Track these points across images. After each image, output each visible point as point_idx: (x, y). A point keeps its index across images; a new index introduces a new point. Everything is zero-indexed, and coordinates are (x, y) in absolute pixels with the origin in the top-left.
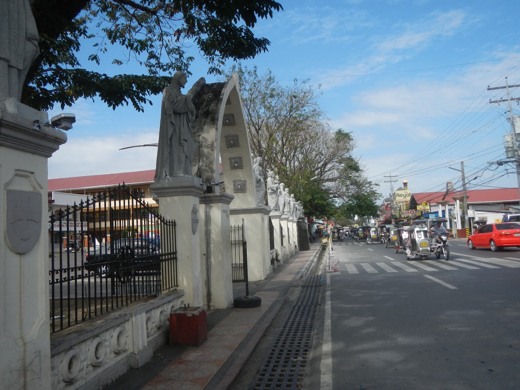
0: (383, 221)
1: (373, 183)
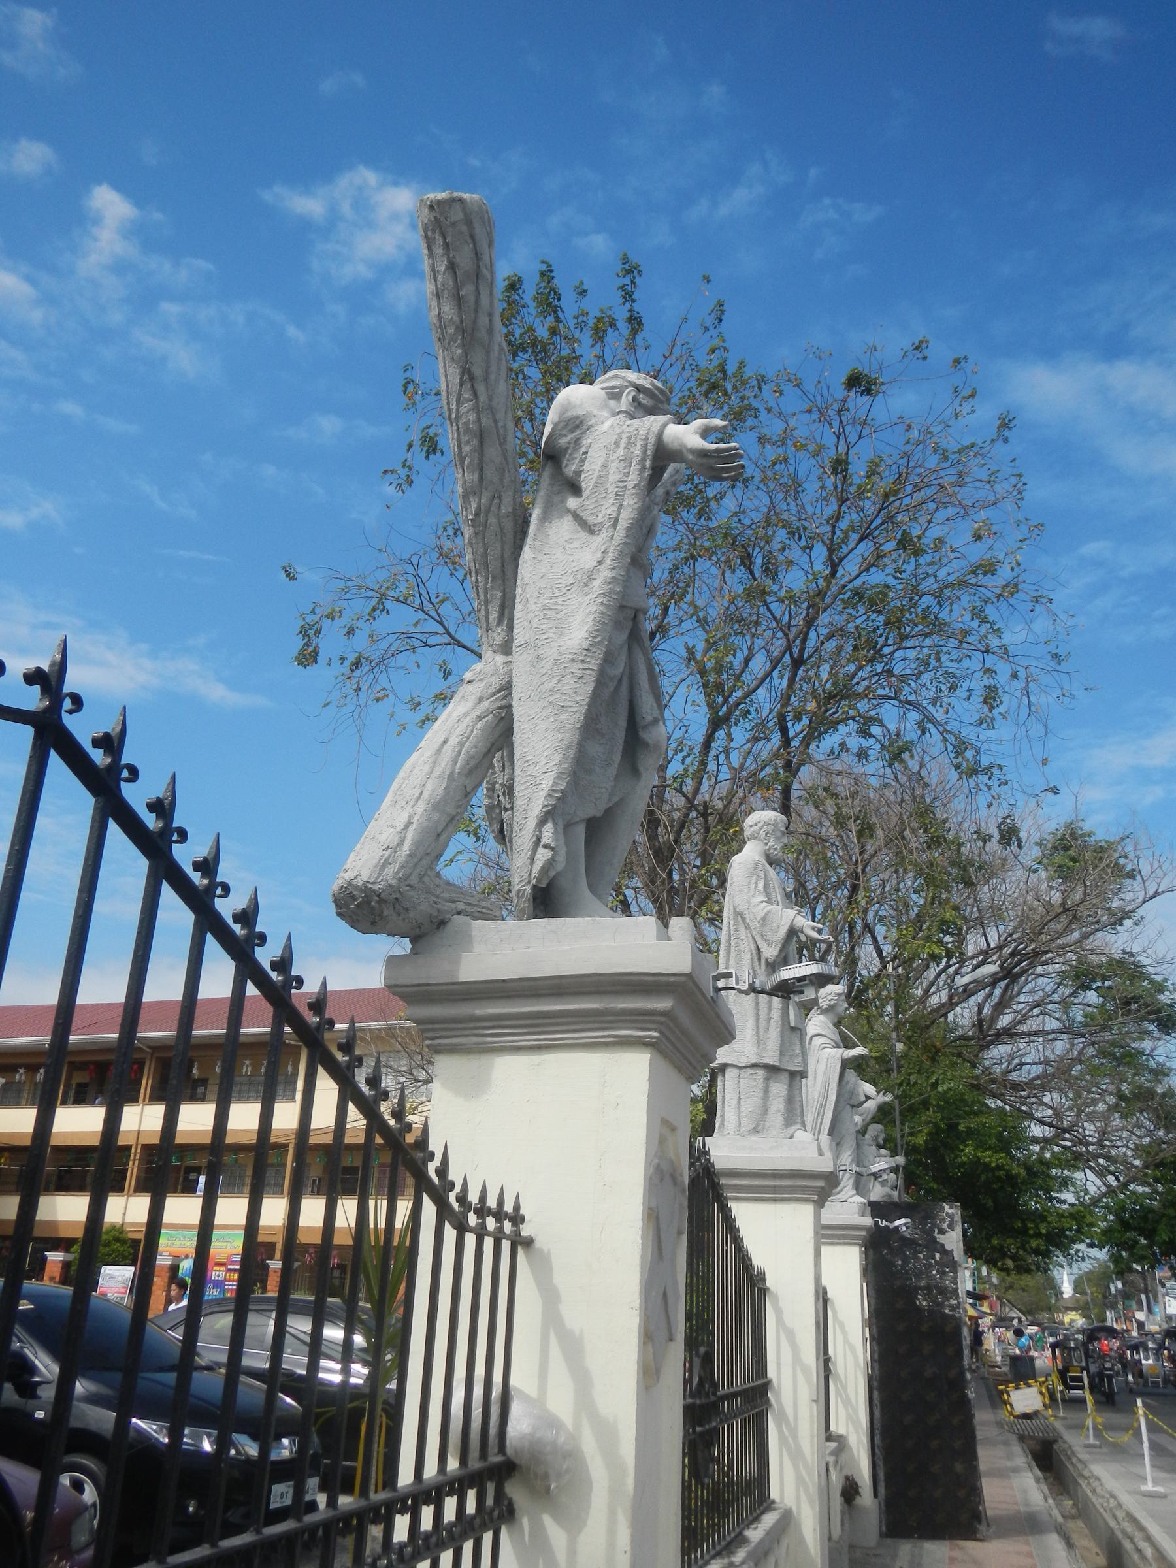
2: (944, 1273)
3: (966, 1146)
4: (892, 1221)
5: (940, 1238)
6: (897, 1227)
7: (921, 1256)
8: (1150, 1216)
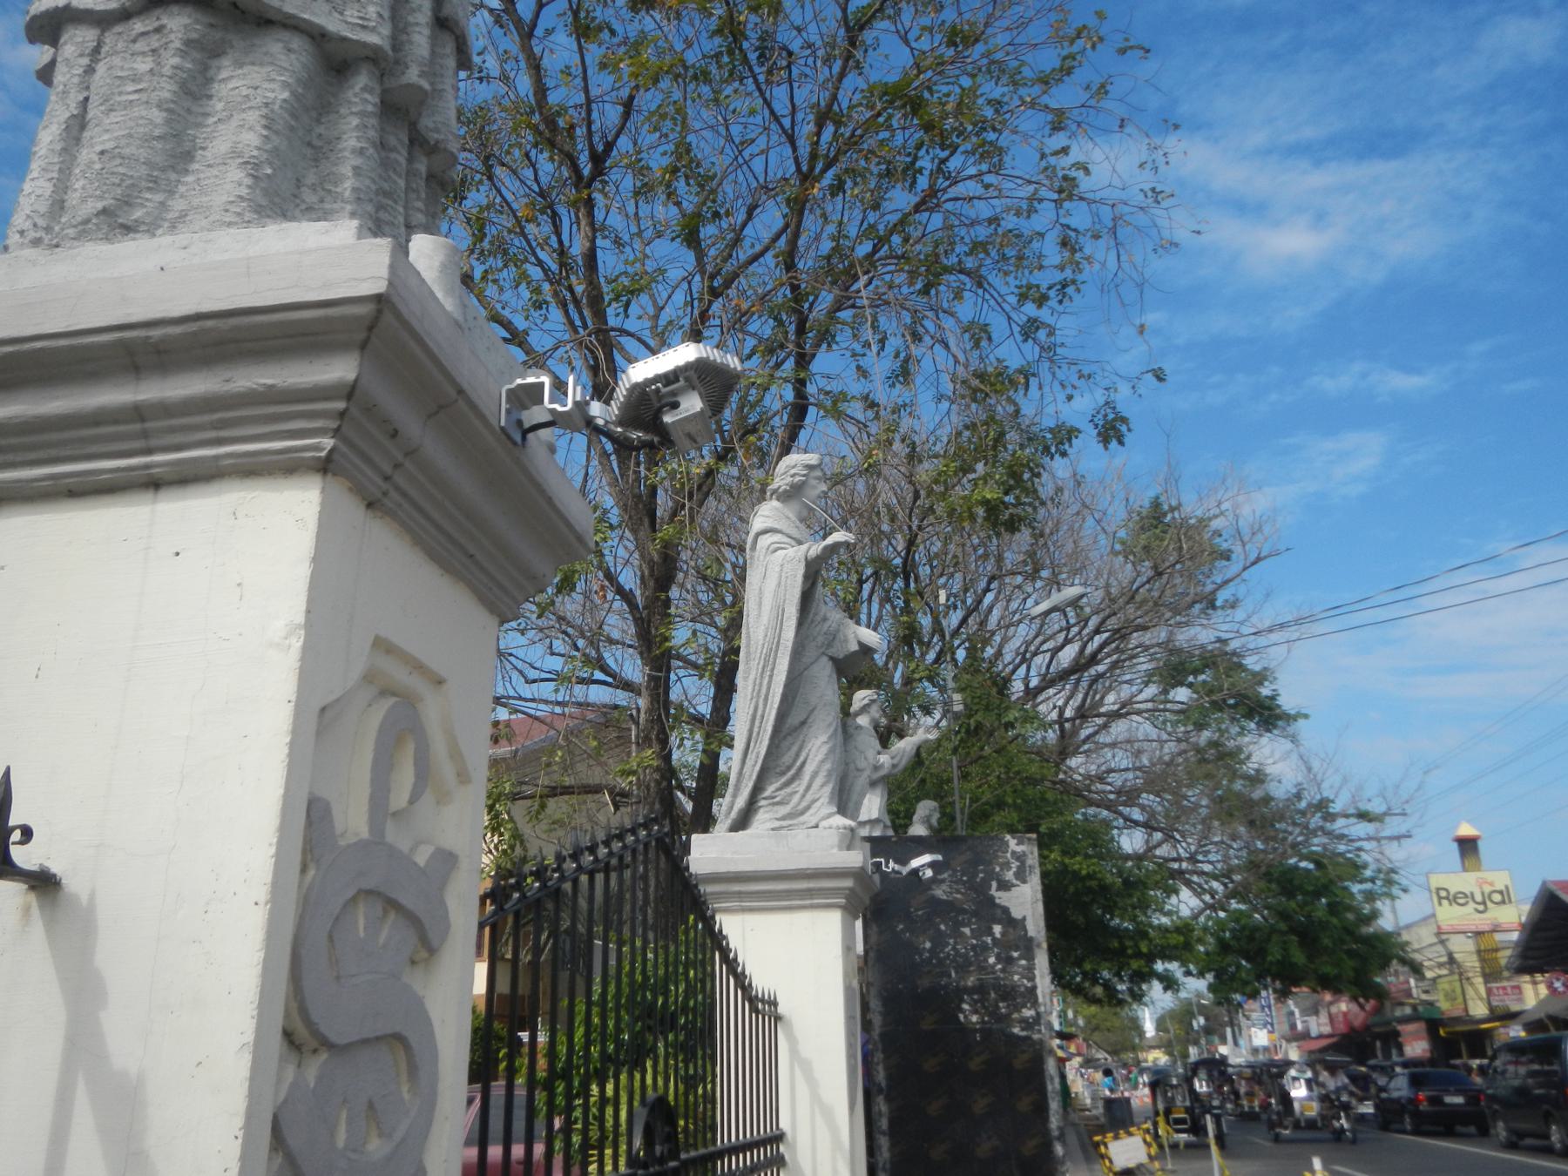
0: (1321, 1036)
1: (1336, 807)
2: (1009, 961)
3: (1051, 851)
4: (904, 862)
5: (1002, 898)
6: (915, 872)
7: (967, 931)
8: (1257, 935)
